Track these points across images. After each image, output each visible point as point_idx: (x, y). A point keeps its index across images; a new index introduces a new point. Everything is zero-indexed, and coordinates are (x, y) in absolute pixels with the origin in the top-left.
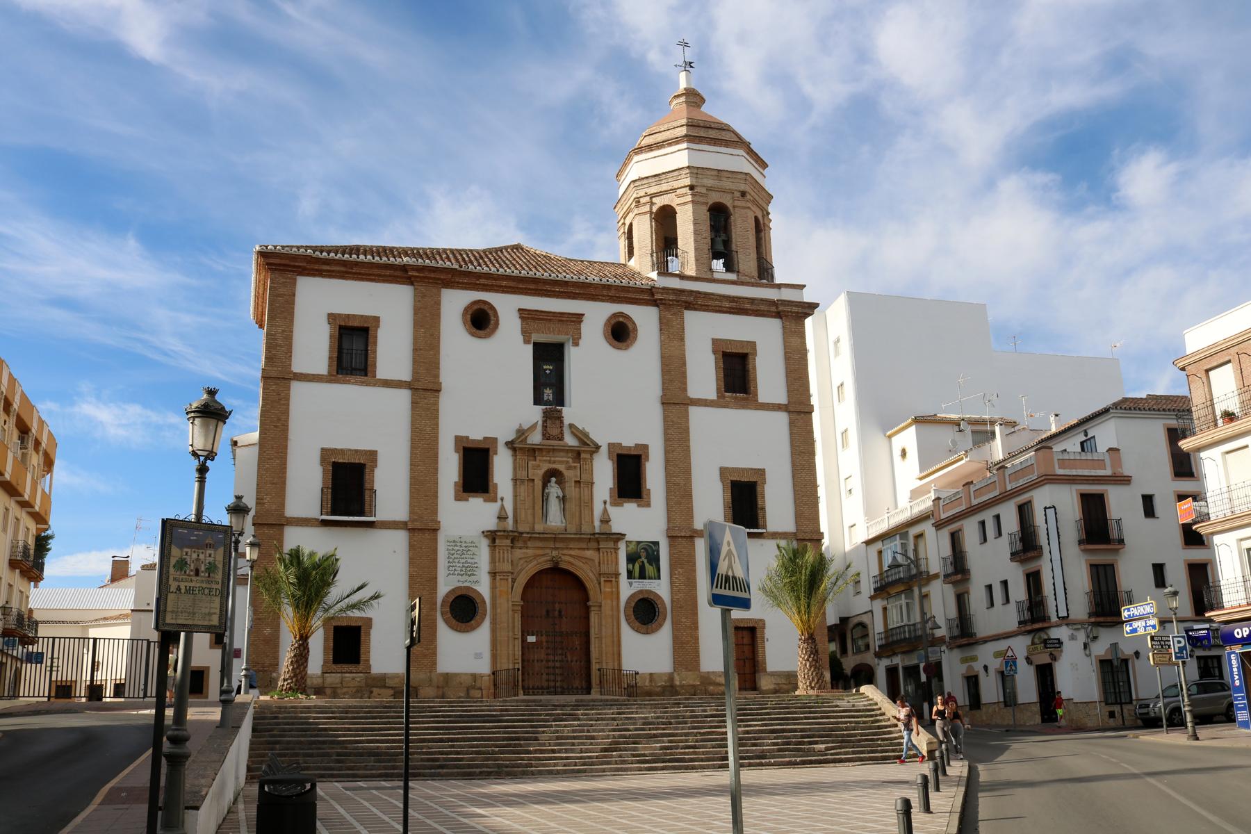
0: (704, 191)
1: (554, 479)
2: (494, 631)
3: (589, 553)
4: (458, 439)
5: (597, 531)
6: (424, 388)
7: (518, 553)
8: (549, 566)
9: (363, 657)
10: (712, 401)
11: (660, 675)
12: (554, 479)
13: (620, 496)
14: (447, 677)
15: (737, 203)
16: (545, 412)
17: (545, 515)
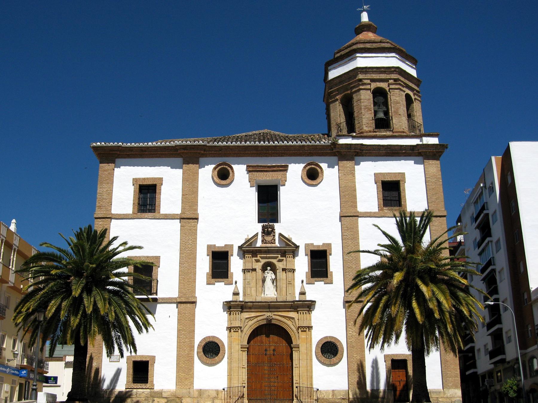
0: (369, 81)
1: (269, 268)
2: (230, 363)
4: (209, 247)
5: (297, 299)
6: (189, 218)
7: (246, 315)
8: (265, 322)
9: (150, 379)
10: (375, 213)
11: (339, 391)
12: (269, 268)
13: (312, 276)
14: (201, 392)
15: (391, 87)
16: (263, 227)
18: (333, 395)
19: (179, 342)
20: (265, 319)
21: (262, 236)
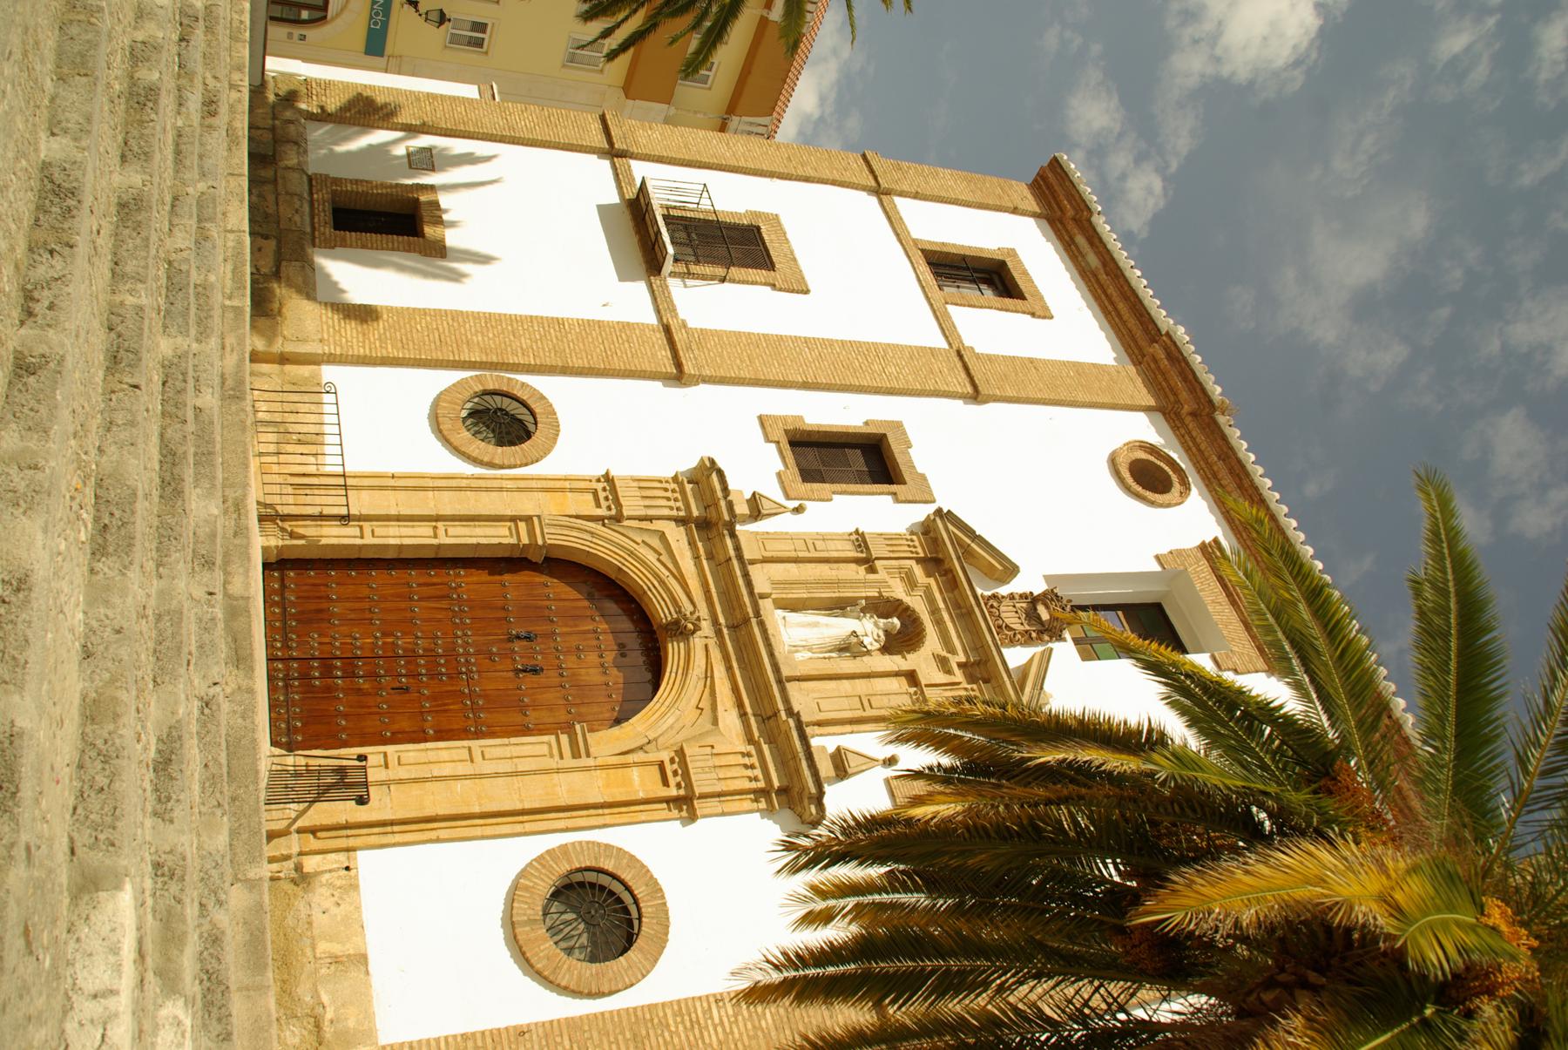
3: (729, 719)
8: (663, 612)
11: (363, 997)
17: (794, 606)
18: (336, 960)
19: (514, 320)
20: (679, 612)
21: (1012, 597)
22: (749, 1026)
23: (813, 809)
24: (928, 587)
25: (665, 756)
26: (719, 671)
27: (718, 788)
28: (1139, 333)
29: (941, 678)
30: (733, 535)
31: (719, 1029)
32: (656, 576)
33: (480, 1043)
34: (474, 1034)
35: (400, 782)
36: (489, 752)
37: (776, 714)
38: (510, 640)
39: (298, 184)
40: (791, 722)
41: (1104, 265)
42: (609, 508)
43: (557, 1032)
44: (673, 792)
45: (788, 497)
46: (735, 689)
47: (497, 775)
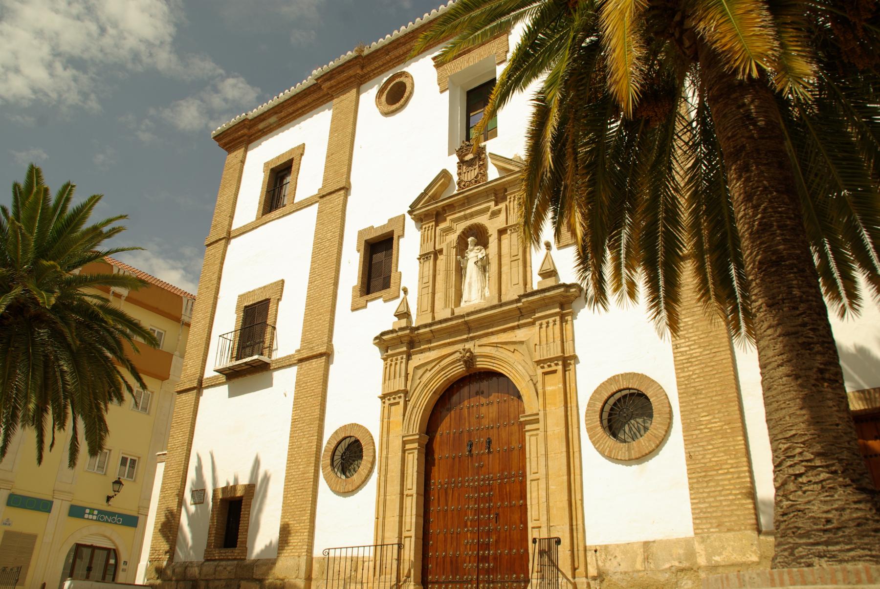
3: (521, 335)
8: (459, 369)
11: (668, 544)
18: (646, 559)
20: (459, 360)
21: (459, 174)
22: (691, 331)
23: (573, 290)
24: (452, 221)
25: (540, 371)
26: (494, 339)
27: (559, 342)
28: (315, 96)
29: (503, 216)
30: (418, 328)
31: (692, 347)
32: (439, 372)
33: (695, 480)
34: (690, 484)
35: (548, 520)
36: (534, 470)
37: (519, 309)
38: (472, 456)
39: (209, 567)
40: (524, 300)
41: (276, 113)
42: (400, 397)
43: (690, 437)
44: (560, 368)
45: (398, 297)
46: (504, 331)
47: (547, 465)
